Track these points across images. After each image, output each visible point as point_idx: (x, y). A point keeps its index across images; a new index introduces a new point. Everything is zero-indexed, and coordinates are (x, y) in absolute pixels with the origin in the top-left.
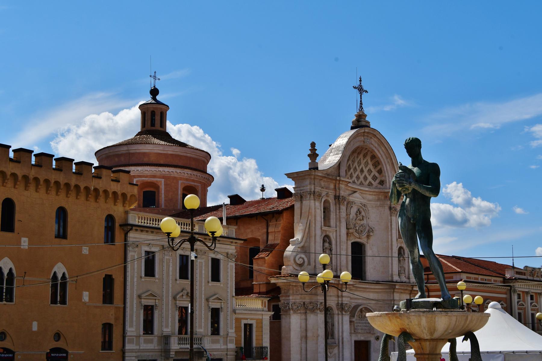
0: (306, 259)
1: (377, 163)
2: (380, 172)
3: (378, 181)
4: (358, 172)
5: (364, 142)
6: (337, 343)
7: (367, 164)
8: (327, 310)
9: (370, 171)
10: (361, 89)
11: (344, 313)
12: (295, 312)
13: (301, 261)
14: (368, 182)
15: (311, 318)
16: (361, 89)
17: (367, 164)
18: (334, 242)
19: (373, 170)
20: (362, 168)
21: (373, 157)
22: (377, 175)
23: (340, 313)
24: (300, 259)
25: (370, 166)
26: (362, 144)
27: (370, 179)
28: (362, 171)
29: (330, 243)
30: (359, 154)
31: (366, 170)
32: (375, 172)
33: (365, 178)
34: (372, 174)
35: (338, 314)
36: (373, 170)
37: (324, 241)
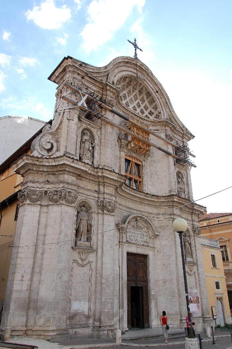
0: (55, 145)
1: (152, 101)
3: (154, 116)
5: (137, 74)
6: (95, 247)
7: (143, 101)
8: (84, 207)
9: (146, 108)
10: (136, 46)
11: (105, 212)
13: (49, 146)
15: (55, 211)
16: (136, 46)
17: (143, 101)
19: (149, 106)
20: (138, 103)
21: (149, 94)
23: (100, 211)
24: (48, 144)
25: (146, 102)
28: (139, 106)
29: (92, 137)
30: (134, 89)
32: (150, 109)
34: (149, 110)
35: (98, 213)
36: (149, 106)
37: (83, 133)
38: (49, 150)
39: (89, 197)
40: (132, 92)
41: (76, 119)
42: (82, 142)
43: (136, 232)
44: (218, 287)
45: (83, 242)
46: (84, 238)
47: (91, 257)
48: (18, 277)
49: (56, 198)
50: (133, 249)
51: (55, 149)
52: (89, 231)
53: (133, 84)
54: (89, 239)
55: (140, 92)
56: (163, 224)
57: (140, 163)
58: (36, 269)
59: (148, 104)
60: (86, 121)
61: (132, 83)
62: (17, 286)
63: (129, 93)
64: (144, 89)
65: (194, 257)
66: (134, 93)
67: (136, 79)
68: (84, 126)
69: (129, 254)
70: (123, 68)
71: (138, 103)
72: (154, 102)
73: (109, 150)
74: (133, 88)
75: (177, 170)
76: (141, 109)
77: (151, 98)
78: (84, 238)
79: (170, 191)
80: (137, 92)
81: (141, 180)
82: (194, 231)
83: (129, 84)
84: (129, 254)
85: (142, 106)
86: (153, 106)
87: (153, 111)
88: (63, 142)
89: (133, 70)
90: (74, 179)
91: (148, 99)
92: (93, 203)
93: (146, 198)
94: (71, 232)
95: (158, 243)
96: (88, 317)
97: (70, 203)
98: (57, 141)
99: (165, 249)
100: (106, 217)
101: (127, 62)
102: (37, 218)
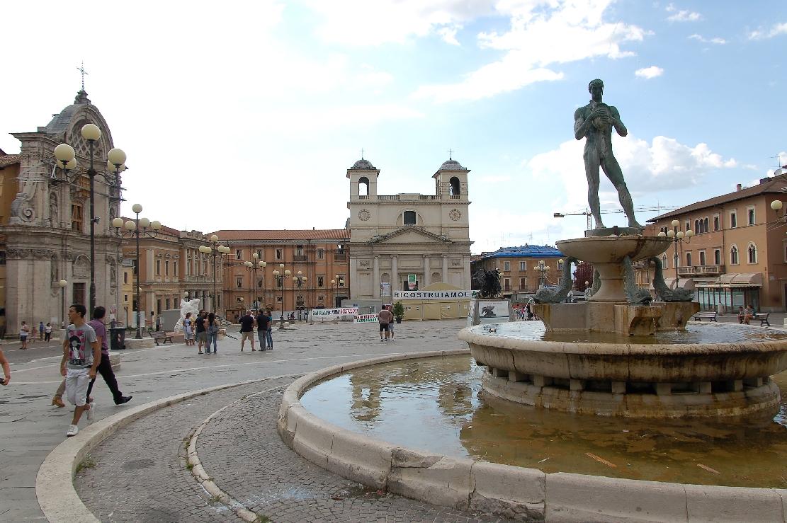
0: (34, 212)
4: (78, 142)
12: (23, 258)
18: (59, 198)
29: (56, 200)
38: (28, 217)
41: (47, 189)
42: (51, 206)
44: (126, 299)
46: (54, 280)
48: (19, 306)
49: (38, 255)
50: (77, 281)
51: (34, 216)
57: (79, 205)
58: (31, 300)
60: (53, 187)
62: (19, 311)
79: (105, 231)
81: (79, 221)
82: (119, 261)
88: (40, 211)
90: (50, 239)
94: (49, 277)
96: (58, 325)
98: (33, 208)
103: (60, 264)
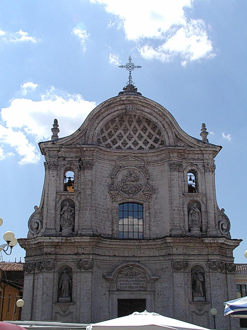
0: (40, 223)
1: (155, 127)
2: (159, 133)
5: (126, 109)
7: (145, 129)
9: (150, 136)
11: (82, 270)
14: (149, 145)
20: (140, 134)
21: (149, 121)
22: (158, 137)
23: (78, 270)
25: (149, 130)
26: (124, 111)
27: (151, 142)
30: (130, 122)
31: (145, 136)
32: (155, 135)
33: (146, 143)
34: (154, 137)
36: (153, 133)
38: (37, 228)
39: (68, 260)
40: (129, 127)
43: (129, 280)
45: (65, 298)
46: (66, 294)
47: (72, 308)
52: (70, 288)
53: (126, 119)
54: (71, 294)
55: (139, 122)
56: (164, 266)
59: (152, 131)
61: (124, 119)
63: (126, 130)
64: (141, 118)
65: (208, 296)
66: (132, 127)
67: (126, 113)
68: (63, 198)
69: (119, 301)
70: (107, 113)
71: (140, 134)
72: (157, 127)
73: (87, 212)
74: (129, 121)
75: (187, 200)
76: (143, 140)
77: (152, 124)
78: (66, 294)
80: (134, 123)
83: (122, 121)
84: (119, 301)
85: (145, 136)
86: (156, 132)
87: (158, 137)
89: (119, 108)
91: (150, 126)
92: (72, 265)
93: (141, 244)
95: (158, 286)
97: (49, 269)
99: (165, 291)
100: (83, 275)
101: (109, 105)
102: (31, 284)
103: (74, 276)
